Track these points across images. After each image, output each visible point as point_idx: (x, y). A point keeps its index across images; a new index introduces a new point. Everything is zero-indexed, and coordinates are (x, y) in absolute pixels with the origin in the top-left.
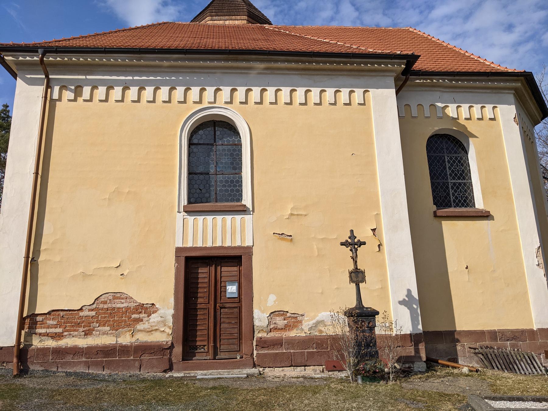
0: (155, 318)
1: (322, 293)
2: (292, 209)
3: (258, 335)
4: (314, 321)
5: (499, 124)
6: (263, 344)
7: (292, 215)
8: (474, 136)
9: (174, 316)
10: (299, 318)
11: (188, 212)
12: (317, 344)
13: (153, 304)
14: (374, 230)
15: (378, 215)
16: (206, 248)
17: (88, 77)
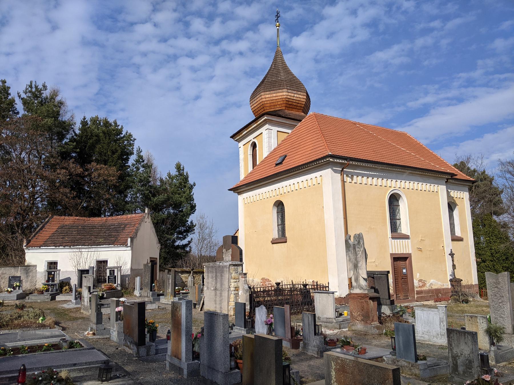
2: (421, 237)
3: (416, 289)
4: (429, 283)
6: (418, 293)
7: (421, 240)
8: (458, 205)
9: (392, 282)
10: (426, 282)
11: (393, 238)
14: (443, 247)
15: (443, 240)
17: (355, 171)
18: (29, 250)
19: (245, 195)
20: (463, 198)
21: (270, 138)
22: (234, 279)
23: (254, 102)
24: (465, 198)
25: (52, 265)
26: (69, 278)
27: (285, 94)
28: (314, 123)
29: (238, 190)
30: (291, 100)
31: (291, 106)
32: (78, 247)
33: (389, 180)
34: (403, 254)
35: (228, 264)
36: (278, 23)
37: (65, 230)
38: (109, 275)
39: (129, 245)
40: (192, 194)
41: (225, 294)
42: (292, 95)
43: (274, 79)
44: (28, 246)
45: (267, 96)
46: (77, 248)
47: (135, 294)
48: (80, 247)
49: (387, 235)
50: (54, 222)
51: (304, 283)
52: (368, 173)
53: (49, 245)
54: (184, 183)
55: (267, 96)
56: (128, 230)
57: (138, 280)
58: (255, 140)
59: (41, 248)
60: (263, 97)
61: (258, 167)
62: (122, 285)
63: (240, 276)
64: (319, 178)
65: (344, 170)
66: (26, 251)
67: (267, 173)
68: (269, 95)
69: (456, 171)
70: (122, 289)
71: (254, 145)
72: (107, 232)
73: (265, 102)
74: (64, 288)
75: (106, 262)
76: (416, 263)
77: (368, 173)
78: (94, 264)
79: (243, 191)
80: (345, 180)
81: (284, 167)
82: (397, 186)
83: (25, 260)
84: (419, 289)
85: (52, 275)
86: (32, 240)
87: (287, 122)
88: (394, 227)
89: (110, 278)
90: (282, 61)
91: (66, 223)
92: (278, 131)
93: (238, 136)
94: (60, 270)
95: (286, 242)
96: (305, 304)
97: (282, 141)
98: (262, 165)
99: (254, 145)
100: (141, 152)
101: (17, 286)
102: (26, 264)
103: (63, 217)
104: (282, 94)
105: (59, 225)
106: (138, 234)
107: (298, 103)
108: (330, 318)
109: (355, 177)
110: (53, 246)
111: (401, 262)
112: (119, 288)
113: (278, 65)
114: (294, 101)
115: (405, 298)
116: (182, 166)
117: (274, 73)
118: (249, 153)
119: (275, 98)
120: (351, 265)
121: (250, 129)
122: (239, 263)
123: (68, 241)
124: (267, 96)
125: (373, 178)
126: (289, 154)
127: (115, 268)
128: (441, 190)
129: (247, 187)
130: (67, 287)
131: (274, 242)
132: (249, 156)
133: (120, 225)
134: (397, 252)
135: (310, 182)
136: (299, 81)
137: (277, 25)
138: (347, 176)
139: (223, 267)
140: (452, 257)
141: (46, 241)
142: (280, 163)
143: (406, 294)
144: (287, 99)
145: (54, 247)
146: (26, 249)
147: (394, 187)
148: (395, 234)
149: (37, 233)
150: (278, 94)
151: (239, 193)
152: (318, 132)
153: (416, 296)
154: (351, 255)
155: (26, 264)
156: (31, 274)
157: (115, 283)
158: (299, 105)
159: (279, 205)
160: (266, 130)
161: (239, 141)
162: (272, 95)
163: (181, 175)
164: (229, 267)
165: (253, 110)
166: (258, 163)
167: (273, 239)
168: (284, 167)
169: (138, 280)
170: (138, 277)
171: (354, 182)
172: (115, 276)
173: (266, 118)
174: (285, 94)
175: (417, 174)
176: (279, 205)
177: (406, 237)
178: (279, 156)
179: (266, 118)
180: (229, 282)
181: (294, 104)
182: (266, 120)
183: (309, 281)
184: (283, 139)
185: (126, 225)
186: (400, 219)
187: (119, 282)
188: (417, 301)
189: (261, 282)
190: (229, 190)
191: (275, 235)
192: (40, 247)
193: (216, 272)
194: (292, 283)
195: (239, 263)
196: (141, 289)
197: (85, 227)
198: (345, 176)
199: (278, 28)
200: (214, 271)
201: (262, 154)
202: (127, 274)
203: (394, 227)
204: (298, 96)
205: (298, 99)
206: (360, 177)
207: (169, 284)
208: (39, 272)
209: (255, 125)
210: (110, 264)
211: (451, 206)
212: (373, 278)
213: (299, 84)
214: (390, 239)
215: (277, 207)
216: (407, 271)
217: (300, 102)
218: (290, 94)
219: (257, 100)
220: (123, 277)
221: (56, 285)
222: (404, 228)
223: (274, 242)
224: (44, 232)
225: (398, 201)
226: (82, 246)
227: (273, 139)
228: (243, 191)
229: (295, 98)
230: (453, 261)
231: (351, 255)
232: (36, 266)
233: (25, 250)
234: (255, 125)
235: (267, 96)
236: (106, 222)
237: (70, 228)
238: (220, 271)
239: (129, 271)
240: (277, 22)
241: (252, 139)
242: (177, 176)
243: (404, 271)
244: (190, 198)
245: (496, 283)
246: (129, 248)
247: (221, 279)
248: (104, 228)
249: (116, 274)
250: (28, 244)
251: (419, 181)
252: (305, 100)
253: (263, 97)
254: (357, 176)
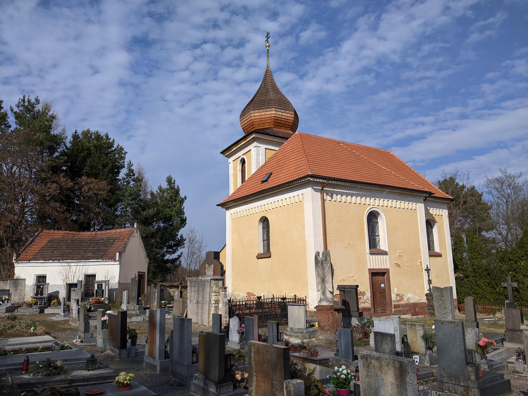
0: (365, 297)
1: (408, 287)
2: (399, 253)
3: (393, 303)
4: (407, 298)
5: (443, 217)
6: (396, 306)
7: (399, 256)
8: (437, 222)
9: (370, 296)
10: (403, 297)
11: (371, 254)
12: (409, 306)
13: (364, 292)
14: (420, 262)
15: (421, 256)
16: (376, 269)
17: (335, 190)
18: (18, 263)
19: (232, 211)
20: (442, 216)
21: (258, 155)
22: (215, 292)
23: (244, 120)
24: (444, 215)
25: (41, 279)
26: (58, 291)
27: (273, 112)
28: (299, 142)
29: (226, 205)
30: (280, 119)
31: (279, 124)
32: (67, 261)
33: (368, 199)
34: (381, 269)
35: (209, 278)
36: (268, 44)
37: (55, 244)
38: (97, 289)
39: (117, 259)
40: (182, 207)
41: (206, 307)
42: (281, 113)
43: (263, 98)
44: (17, 260)
45: (256, 114)
46: (66, 262)
47: (122, 308)
48: (69, 261)
49: (366, 251)
50: (44, 236)
51: (284, 297)
52: (348, 191)
53: (38, 259)
54: (175, 197)
55: (256, 115)
56: (117, 244)
57: (125, 293)
58: (244, 157)
59: (31, 261)
60: (252, 115)
61: (246, 183)
62: (110, 299)
63: (221, 290)
64: (301, 196)
65: (324, 189)
66: (15, 265)
67: (254, 190)
68: (258, 114)
69: (436, 189)
70: (109, 303)
71: (243, 162)
72: (96, 246)
73: (255, 121)
74: (53, 302)
75: (94, 276)
77: (348, 191)
78: (82, 278)
79: (231, 207)
80: (325, 199)
81: (269, 184)
82: (376, 204)
83: (14, 273)
84: (397, 303)
85: (41, 288)
86: (21, 254)
87: (275, 140)
88: (373, 243)
89: (98, 292)
90: (272, 81)
91: (55, 237)
93: (227, 152)
94: (49, 284)
95: (270, 257)
96: (283, 317)
97: (269, 159)
98: (250, 182)
99: (243, 162)
100: (132, 166)
101: (5, 299)
102: (15, 278)
103: (52, 231)
104: (271, 113)
105: (49, 239)
106: (127, 248)
107: (286, 122)
108: (301, 329)
109: (335, 195)
110: (43, 260)
111: (380, 277)
112: (107, 302)
113: (267, 84)
114: (283, 120)
115: (383, 311)
116: (173, 180)
117: (263, 92)
118: (238, 169)
119: (263, 117)
120: (319, 279)
121: (239, 146)
122: (220, 277)
123: (57, 255)
124: (256, 115)
125: (352, 197)
126: (274, 172)
127: (102, 281)
128: (420, 207)
129: (234, 202)
130: (55, 301)
131: (259, 257)
132: (238, 171)
133: (109, 239)
134: (375, 268)
135: (292, 199)
136: (287, 100)
137: (267, 46)
138: (327, 194)
139: (205, 281)
140: (428, 272)
141: (35, 255)
142: (266, 181)
143: (384, 308)
144: (275, 118)
145: (43, 261)
146: (15, 263)
147: (373, 205)
148: (373, 250)
149: (27, 247)
150: (267, 113)
151: (227, 209)
152: (301, 152)
153: (393, 310)
154: (319, 270)
155: (15, 278)
156: (20, 287)
157: (103, 297)
158: (287, 123)
159: (265, 221)
160: (254, 147)
161: (229, 156)
162: (261, 114)
163: (172, 188)
164: (210, 281)
165: (243, 127)
166: (246, 179)
167: (258, 254)
168: (269, 184)
169: (125, 293)
170: (126, 291)
171: (333, 200)
172: (103, 290)
173: (254, 136)
174: (273, 112)
175: (395, 192)
176: (265, 221)
177: (385, 253)
178: (265, 173)
179: (254, 136)
180: (210, 295)
181: (283, 122)
182: (254, 137)
183: (290, 295)
184: (270, 156)
185: (114, 240)
186: (379, 236)
187: (107, 296)
188: (394, 315)
189: (246, 297)
190: (217, 205)
191: (261, 250)
192: (29, 261)
193: (198, 286)
194: (273, 296)
195: (220, 277)
196: (128, 303)
197: (75, 242)
198: (325, 194)
199: (268, 48)
200: (197, 285)
201: (250, 170)
202: (115, 288)
203: (373, 243)
204: (286, 114)
205: (286, 118)
206: (339, 196)
207: (155, 298)
208: (28, 285)
209: (244, 142)
210: (98, 279)
211: (430, 223)
212: (344, 291)
213: (287, 103)
214: (368, 255)
215: (263, 223)
216: (385, 285)
217: (288, 121)
218: (278, 113)
219: (247, 118)
220: (111, 291)
221: (44, 298)
222: (383, 245)
223: (259, 257)
224: (34, 246)
225: (377, 218)
226: (71, 260)
227: (261, 156)
228: (231, 207)
229: (283, 117)
230: (429, 276)
231: (319, 270)
232: (25, 279)
233: (15, 264)
234: (244, 142)
235: (256, 114)
236: (96, 236)
237: (59, 243)
238: (201, 285)
239: (117, 285)
240: (267, 43)
241: (241, 155)
242: (168, 190)
243: (382, 285)
244: (181, 212)
245: (440, 296)
246: (118, 263)
247: (203, 292)
248: (93, 243)
249: (103, 288)
250: (17, 257)
251: (397, 199)
252: (293, 119)
253: (252, 115)
254: (337, 195)
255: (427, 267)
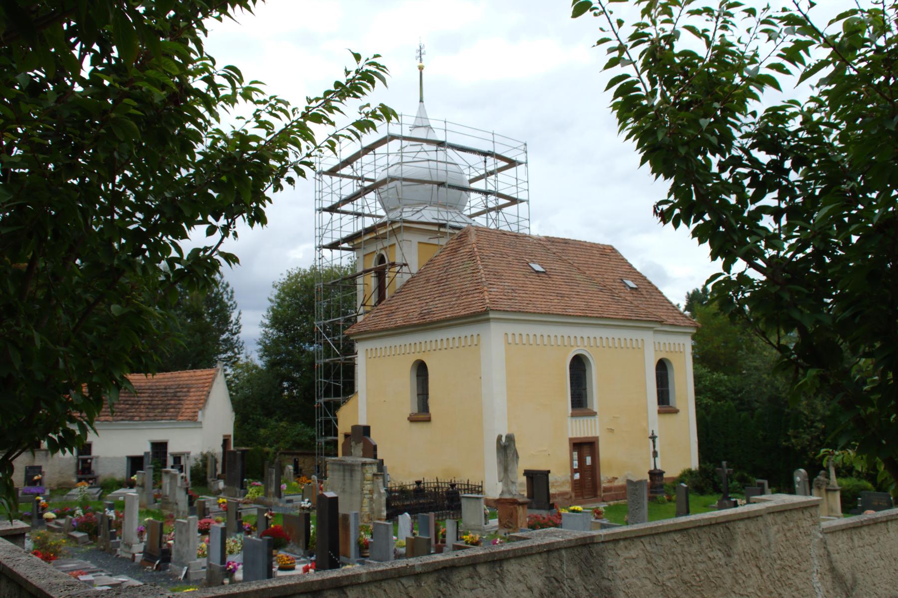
6: (606, 490)
34: (587, 438)
51: (453, 482)
56: (193, 395)
58: (383, 252)
76: (605, 452)
78: (148, 448)
92: (419, 243)
207: (271, 481)
210: (172, 449)
223: (413, 419)
230: (654, 446)
255: (653, 434)
